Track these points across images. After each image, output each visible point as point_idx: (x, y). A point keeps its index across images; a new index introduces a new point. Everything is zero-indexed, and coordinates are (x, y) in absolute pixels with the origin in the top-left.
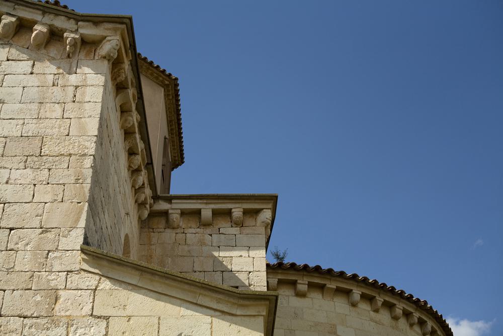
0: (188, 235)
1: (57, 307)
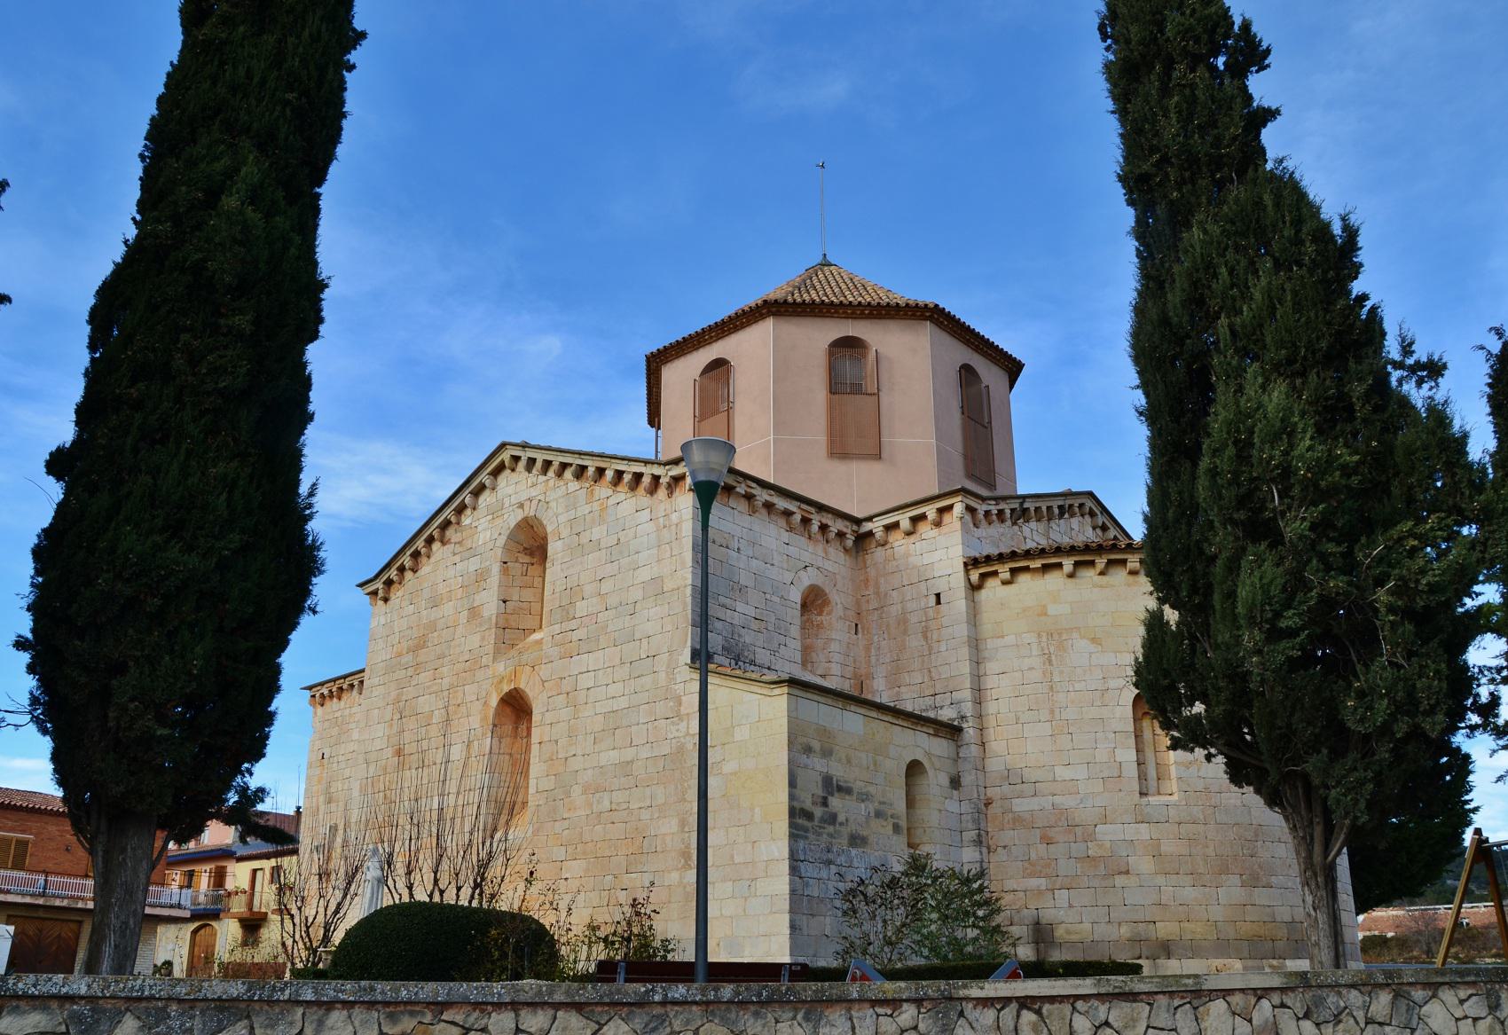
1: (682, 708)
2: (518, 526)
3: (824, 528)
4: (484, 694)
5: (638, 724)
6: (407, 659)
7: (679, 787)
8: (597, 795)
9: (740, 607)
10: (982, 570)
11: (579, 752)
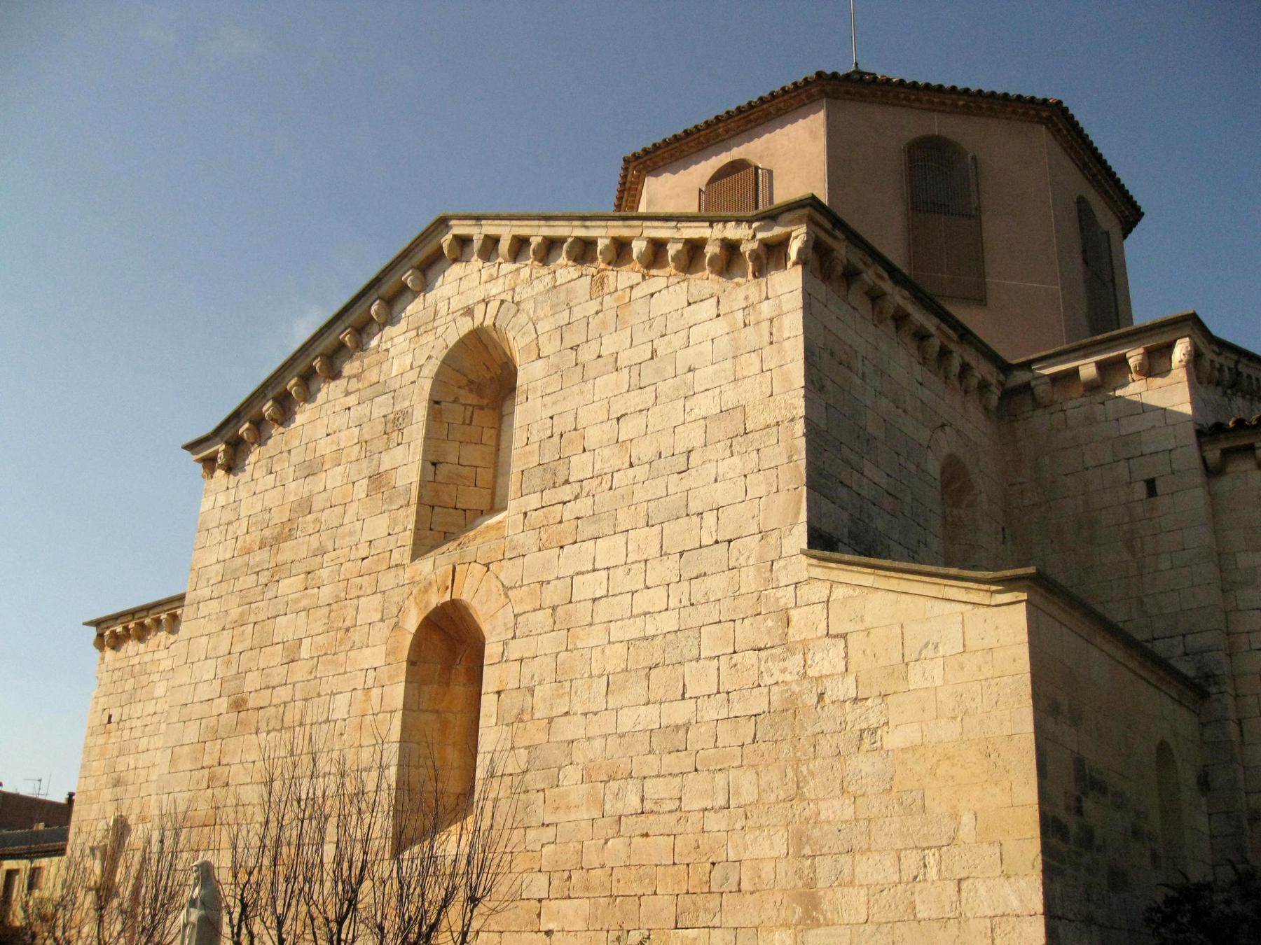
0: (1069, 413)
1: (791, 631)
2: (462, 342)
3: (965, 368)
4: (394, 610)
5: (698, 659)
6: (260, 557)
7: (790, 773)
8: (614, 785)
9: (869, 469)
10: (1225, 445)
11: (578, 708)
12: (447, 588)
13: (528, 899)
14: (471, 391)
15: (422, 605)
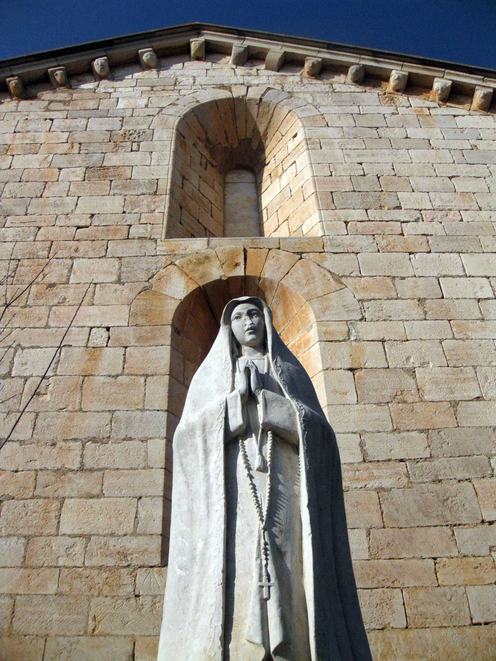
12: (237, 265)
13: (486, 624)
14: (206, 147)
15: (196, 275)
